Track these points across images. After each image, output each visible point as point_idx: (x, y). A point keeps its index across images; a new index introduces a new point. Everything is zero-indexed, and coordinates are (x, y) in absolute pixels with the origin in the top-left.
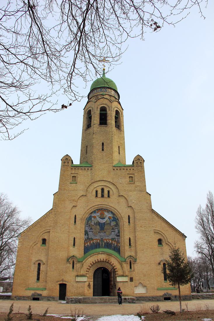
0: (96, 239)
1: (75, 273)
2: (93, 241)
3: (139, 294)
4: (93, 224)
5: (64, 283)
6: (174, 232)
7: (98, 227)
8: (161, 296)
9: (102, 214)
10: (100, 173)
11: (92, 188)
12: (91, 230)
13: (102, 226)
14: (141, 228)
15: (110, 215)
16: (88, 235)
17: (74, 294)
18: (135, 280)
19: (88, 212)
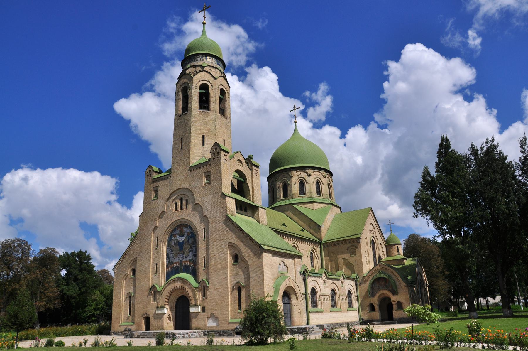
0: (176, 263)
1: (155, 305)
2: (173, 265)
3: (211, 327)
4: (173, 244)
5: (148, 316)
6: (251, 243)
7: (178, 247)
8: (232, 330)
9: (181, 231)
10: (178, 179)
11: (171, 200)
12: (172, 252)
13: (181, 246)
14: (215, 243)
15: (188, 231)
16: (169, 259)
17: (155, 327)
18: (208, 310)
19: (167, 230)
